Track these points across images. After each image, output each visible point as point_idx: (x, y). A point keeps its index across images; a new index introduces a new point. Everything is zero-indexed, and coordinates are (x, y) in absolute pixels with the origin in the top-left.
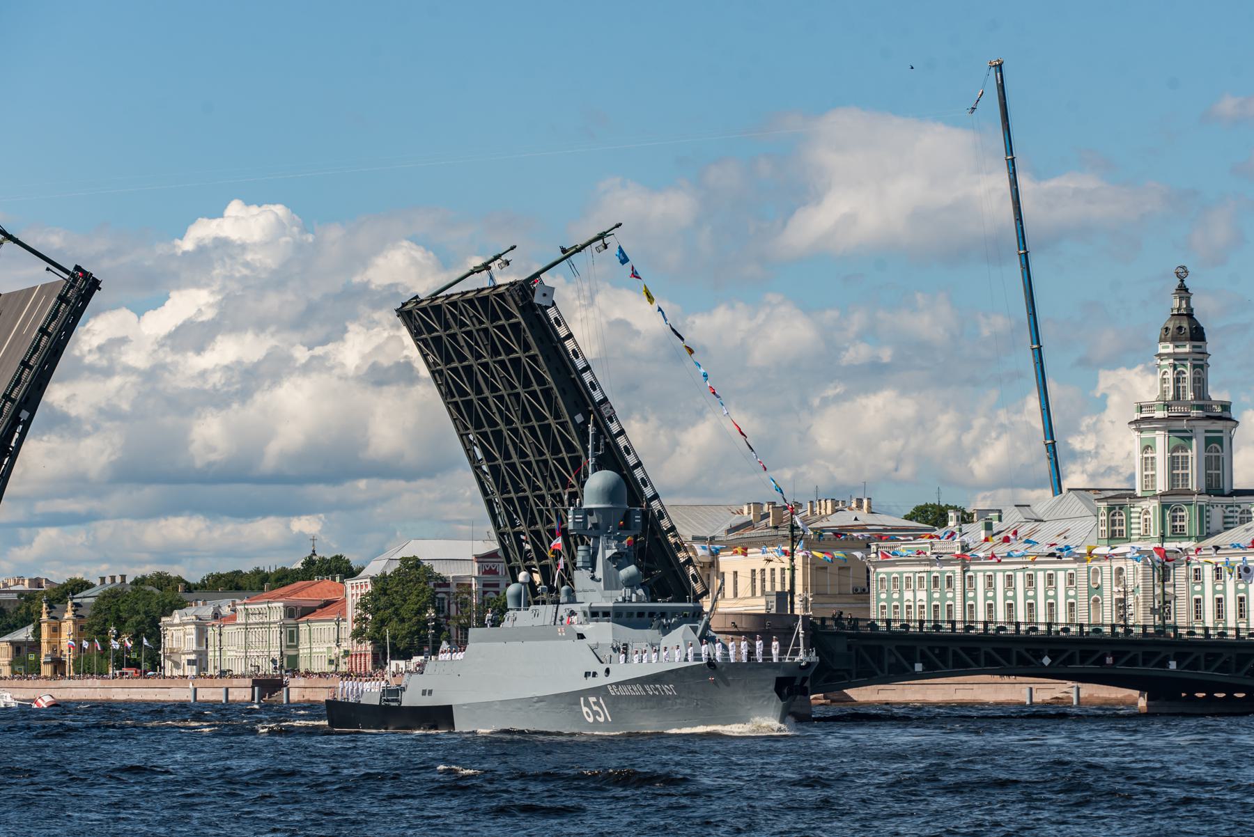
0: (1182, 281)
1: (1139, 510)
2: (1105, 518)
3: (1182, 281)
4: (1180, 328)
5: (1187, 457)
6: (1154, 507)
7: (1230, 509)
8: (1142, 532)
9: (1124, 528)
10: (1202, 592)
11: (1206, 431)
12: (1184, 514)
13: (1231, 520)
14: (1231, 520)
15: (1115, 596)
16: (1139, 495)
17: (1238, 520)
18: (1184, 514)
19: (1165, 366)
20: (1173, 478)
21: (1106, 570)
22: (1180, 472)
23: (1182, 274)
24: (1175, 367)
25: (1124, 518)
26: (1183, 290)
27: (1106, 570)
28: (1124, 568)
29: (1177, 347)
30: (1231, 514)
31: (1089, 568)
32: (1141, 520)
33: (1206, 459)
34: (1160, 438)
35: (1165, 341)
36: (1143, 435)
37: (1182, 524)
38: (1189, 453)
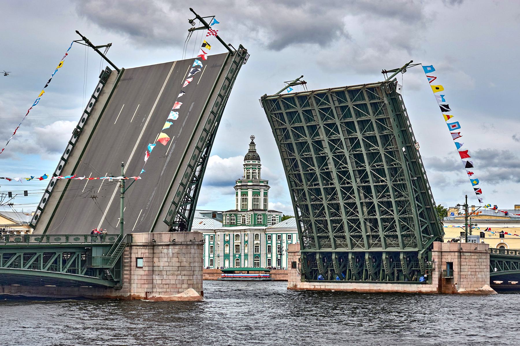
0: (252, 140)
1: (241, 215)
2: (229, 218)
3: (252, 140)
4: (254, 155)
5: (258, 198)
6: (252, 215)
7: (270, 216)
8: (241, 223)
9: (235, 221)
10: (271, 243)
11: (264, 190)
12: (261, 217)
13: (270, 220)
14: (270, 220)
15: (235, 244)
16: (240, 210)
17: (271, 220)
18: (261, 217)
19: (250, 168)
20: (253, 205)
21: (232, 236)
22: (256, 203)
23: (253, 138)
24: (252, 168)
25: (235, 218)
26: (252, 143)
27: (232, 236)
28: (240, 235)
29: (253, 162)
30: (270, 218)
31: (245, 234)
32: (241, 219)
33: (264, 199)
34: (250, 192)
35: (248, 160)
36: (242, 191)
37: (261, 220)
38: (259, 197)
